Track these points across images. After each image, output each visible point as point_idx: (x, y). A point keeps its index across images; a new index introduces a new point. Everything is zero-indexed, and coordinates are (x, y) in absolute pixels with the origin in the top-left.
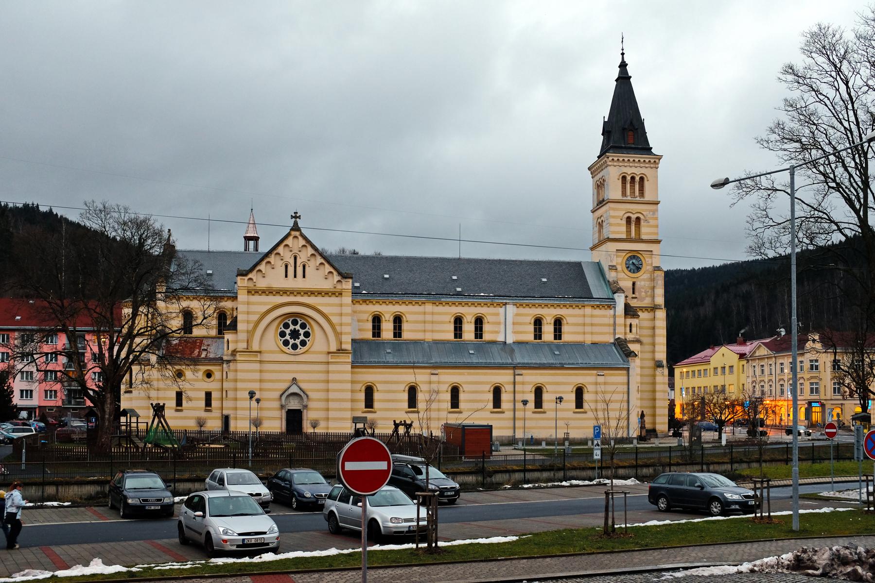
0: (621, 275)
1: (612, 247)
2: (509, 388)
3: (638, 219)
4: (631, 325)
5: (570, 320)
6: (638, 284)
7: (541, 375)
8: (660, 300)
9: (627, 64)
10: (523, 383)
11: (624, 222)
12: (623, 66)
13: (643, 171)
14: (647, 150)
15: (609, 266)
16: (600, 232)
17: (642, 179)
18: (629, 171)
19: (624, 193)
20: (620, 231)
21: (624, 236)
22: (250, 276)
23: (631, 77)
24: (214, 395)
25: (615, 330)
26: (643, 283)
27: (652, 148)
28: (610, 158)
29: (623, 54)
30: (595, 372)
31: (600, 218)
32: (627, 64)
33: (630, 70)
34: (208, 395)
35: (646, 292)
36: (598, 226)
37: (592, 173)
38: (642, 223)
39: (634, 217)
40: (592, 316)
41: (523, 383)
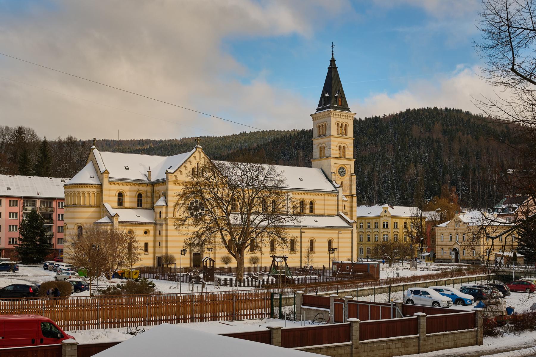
0: (337, 177)
1: (333, 161)
2: (299, 240)
3: (344, 147)
4: (345, 205)
5: (318, 202)
6: (344, 182)
7: (313, 233)
8: (354, 192)
9: (335, 60)
10: (305, 237)
11: (338, 148)
12: (333, 61)
13: (347, 121)
14: (348, 109)
15: (332, 172)
16: (320, 151)
17: (346, 125)
18: (341, 120)
19: (338, 134)
20: (335, 152)
21: (338, 156)
22: (175, 174)
23: (337, 68)
24: (151, 245)
25: (338, 208)
26: (346, 182)
27: (350, 108)
28: (332, 113)
29: (333, 54)
30: (337, 231)
31: (322, 144)
32: (335, 60)
33: (337, 64)
34: (146, 245)
35: (347, 187)
36: (318, 149)
37: (313, 118)
38: (346, 148)
39: (342, 146)
40: (328, 200)
41: (305, 237)
